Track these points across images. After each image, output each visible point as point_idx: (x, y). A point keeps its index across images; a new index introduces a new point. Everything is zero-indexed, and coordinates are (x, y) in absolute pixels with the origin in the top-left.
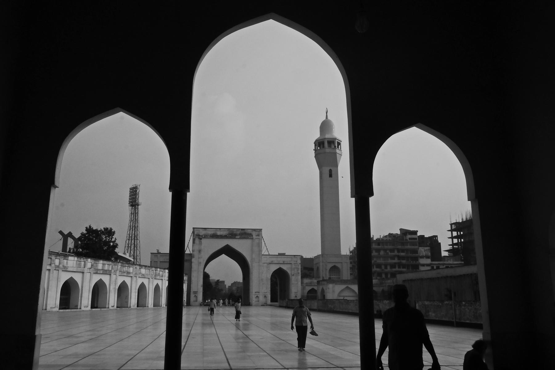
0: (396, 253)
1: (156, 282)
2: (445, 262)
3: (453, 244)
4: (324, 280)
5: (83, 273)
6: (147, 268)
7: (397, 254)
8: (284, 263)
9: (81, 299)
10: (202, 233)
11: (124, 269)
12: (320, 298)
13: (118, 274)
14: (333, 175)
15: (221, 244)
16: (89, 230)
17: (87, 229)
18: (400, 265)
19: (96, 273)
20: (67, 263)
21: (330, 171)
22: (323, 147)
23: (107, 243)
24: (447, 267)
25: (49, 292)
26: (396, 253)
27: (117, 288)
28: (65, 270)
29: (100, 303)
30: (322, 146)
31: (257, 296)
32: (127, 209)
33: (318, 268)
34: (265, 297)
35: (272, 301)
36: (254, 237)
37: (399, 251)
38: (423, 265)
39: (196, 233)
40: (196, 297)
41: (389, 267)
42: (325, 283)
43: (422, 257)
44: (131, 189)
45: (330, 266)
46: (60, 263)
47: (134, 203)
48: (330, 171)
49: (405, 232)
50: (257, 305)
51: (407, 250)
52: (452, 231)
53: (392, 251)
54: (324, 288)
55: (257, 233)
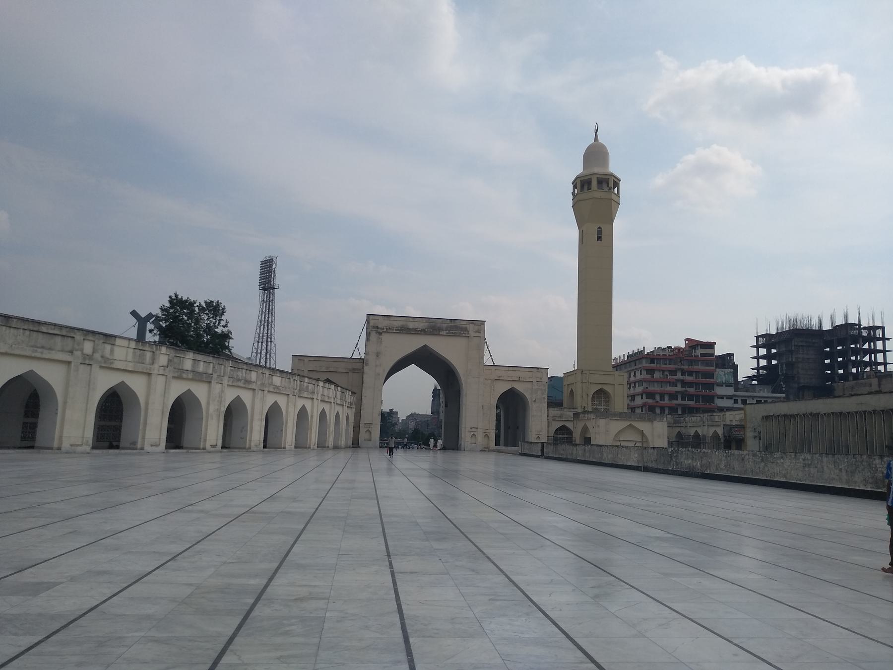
0: (679, 376)
1: (300, 403)
2: (755, 394)
3: (758, 368)
4: (585, 412)
5: (149, 374)
6: (284, 375)
7: (681, 378)
9: (145, 430)
10: (383, 324)
11: (240, 374)
12: (578, 442)
13: (226, 381)
15: (413, 344)
16: (177, 303)
17: (171, 301)
18: (684, 396)
19: (179, 378)
20: (112, 351)
22: (590, 189)
23: (209, 329)
24: (759, 402)
25: (68, 412)
26: (679, 376)
27: (224, 409)
28: (108, 365)
29: (188, 437)
30: (586, 187)
32: (256, 294)
33: (572, 391)
34: (487, 436)
35: (497, 443)
36: (472, 333)
37: (683, 374)
38: (721, 397)
39: (372, 324)
41: (666, 398)
42: (592, 416)
43: (720, 385)
44: (263, 263)
46: (94, 351)
47: (267, 285)
49: (693, 344)
50: (472, 450)
51: (697, 372)
52: (758, 347)
53: (673, 372)
54: (590, 425)
55: (476, 327)
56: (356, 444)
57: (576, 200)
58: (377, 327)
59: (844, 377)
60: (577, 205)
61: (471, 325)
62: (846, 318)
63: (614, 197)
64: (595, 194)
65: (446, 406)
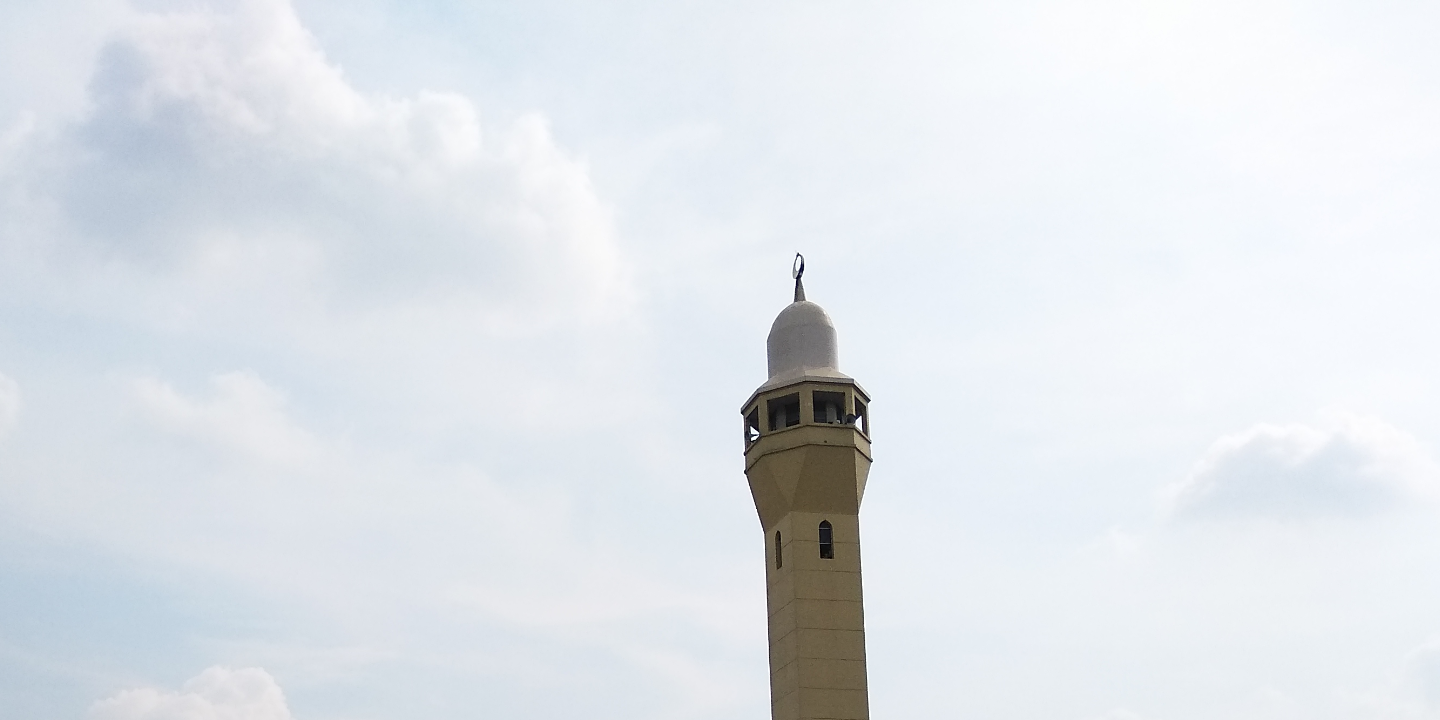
14: (836, 549)
21: (826, 530)
22: (793, 419)
30: (782, 419)
48: (826, 530)
57: (756, 452)
60: (757, 468)
63: (858, 441)
64: (806, 433)
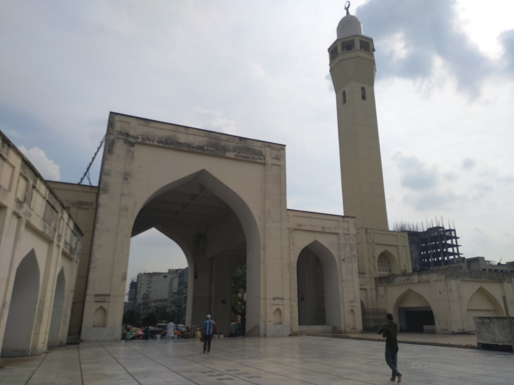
8: (323, 232)
10: (136, 130)
15: (182, 167)
31: (278, 310)
39: (118, 127)
40: (104, 311)
45: (379, 250)
56: (75, 337)
58: (124, 134)
59: (438, 263)
61: (268, 149)
62: (432, 225)
65: (195, 276)
